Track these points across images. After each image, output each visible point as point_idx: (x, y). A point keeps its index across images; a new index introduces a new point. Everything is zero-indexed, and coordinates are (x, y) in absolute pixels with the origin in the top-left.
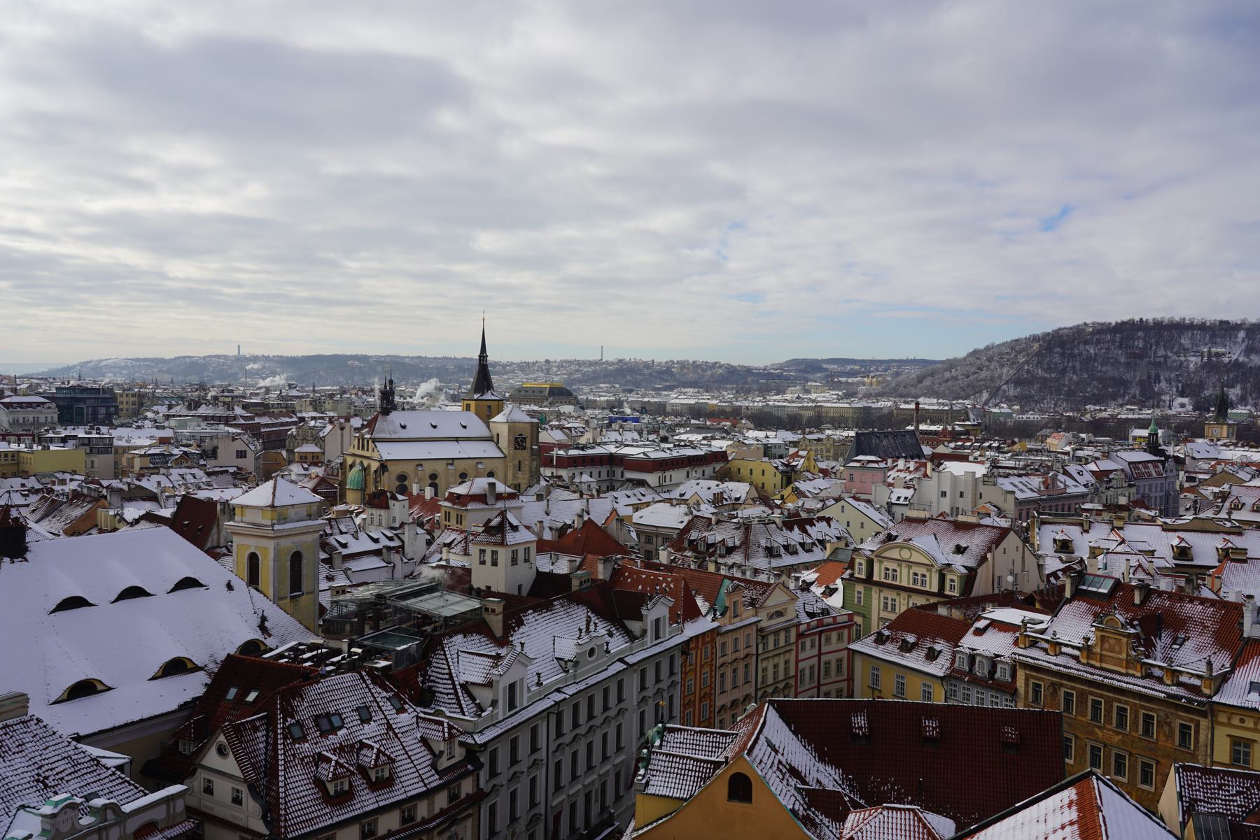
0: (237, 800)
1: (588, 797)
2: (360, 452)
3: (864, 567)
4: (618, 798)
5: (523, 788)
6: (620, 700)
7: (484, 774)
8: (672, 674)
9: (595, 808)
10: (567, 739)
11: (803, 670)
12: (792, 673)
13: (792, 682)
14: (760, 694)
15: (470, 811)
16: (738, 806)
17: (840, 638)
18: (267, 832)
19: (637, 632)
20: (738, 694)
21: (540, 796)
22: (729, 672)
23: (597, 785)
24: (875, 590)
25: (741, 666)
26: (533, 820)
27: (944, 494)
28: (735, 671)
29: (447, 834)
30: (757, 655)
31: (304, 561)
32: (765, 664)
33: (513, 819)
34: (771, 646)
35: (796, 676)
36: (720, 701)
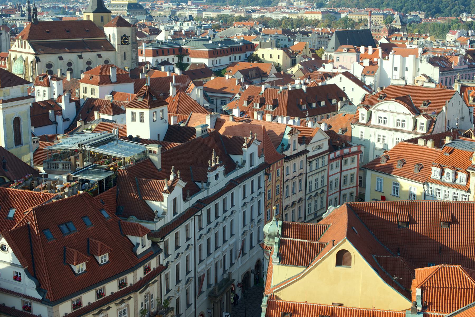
0: (17, 278)
1: (216, 265)
2: (20, 49)
3: (366, 117)
4: (232, 264)
5: (182, 261)
6: (232, 206)
7: (162, 255)
8: (260, 187)
9: (220, 271)
10: (204, 231)
11: (332, 182)
12: (325, 183)
13: (325, 189)
14: (308, 197)
15: (156, 279)
16: (342, 269)
17: (353, 161)
18: (41, 298)
19: (240, 163)
20: (295, 198)
21: (192, 267)
22: (290, 184)
23: (221, 258)
24: (372, 130)
25: (297, 180)
26: (188, 281)
27: (396, 69)
28: (294, 184)
29: (144, 294)
30: (306, 173)
31: (22, 123)
32: (311, 178)
33: (178, 281)
34: (314, 168)
35: (328, 185)
36: (287, 202)
